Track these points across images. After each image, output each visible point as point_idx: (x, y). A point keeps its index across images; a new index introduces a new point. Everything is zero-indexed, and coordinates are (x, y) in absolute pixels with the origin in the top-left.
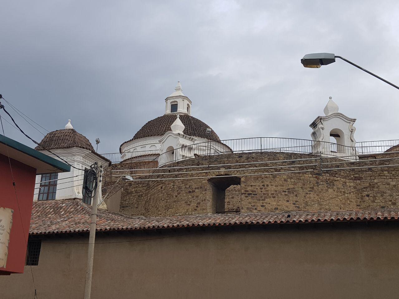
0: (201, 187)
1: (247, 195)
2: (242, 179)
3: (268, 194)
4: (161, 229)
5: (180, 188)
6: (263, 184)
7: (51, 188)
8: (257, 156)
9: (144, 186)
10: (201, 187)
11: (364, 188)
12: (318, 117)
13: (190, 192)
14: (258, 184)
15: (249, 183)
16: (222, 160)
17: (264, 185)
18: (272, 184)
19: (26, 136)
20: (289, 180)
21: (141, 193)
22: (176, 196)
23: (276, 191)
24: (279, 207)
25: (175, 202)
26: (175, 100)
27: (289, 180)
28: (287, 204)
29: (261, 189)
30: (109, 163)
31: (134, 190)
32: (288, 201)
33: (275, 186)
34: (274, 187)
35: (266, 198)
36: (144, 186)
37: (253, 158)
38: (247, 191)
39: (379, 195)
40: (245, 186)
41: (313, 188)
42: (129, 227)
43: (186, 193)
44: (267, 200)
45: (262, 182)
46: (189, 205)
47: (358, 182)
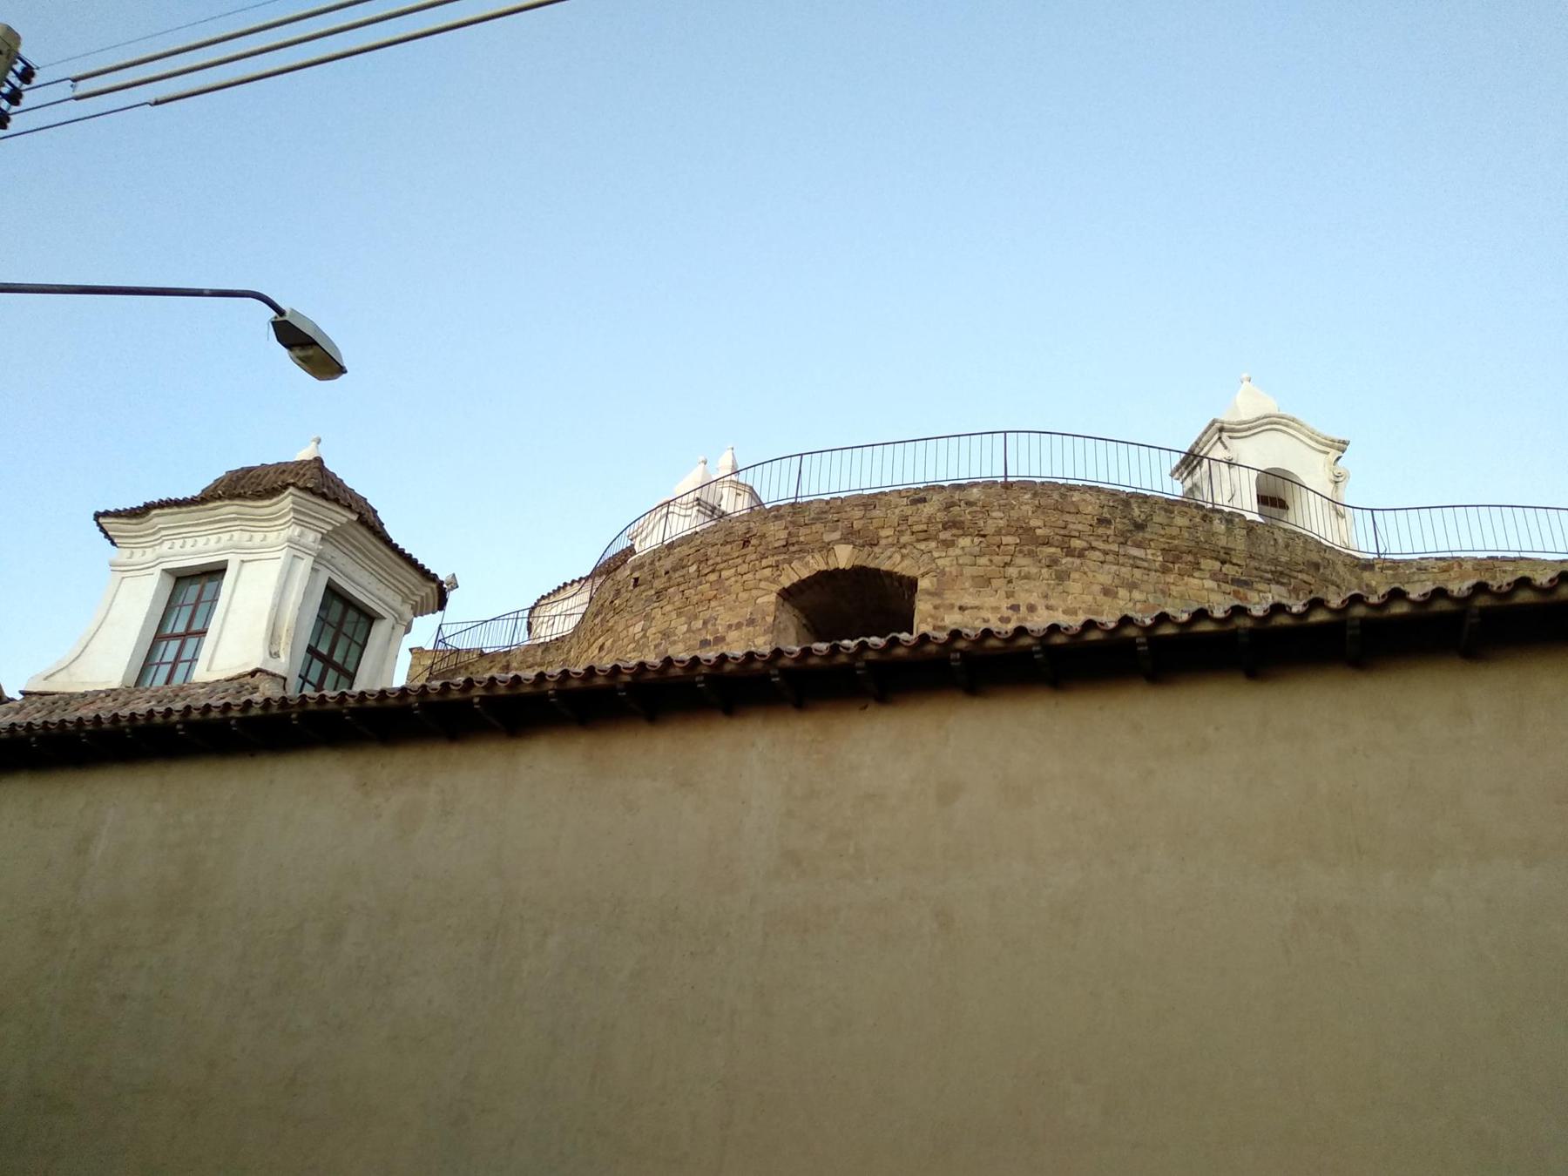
0: (751, 622)
2: (923, 584)
6: (1012, 601)
7: (191, 642)
8: (988, 496)
10: (751, 622)
12: (1214, 422)
14: (991, 601)
15: (950, 597)
16: (844, 515)
17: (1015, 608)
18: (1052, 602)
20: (1122, 592)
27: (1122, 592)
33: (1064, 612)
37: (969, 504)
40: (936, 607)
45: (1009, 595)
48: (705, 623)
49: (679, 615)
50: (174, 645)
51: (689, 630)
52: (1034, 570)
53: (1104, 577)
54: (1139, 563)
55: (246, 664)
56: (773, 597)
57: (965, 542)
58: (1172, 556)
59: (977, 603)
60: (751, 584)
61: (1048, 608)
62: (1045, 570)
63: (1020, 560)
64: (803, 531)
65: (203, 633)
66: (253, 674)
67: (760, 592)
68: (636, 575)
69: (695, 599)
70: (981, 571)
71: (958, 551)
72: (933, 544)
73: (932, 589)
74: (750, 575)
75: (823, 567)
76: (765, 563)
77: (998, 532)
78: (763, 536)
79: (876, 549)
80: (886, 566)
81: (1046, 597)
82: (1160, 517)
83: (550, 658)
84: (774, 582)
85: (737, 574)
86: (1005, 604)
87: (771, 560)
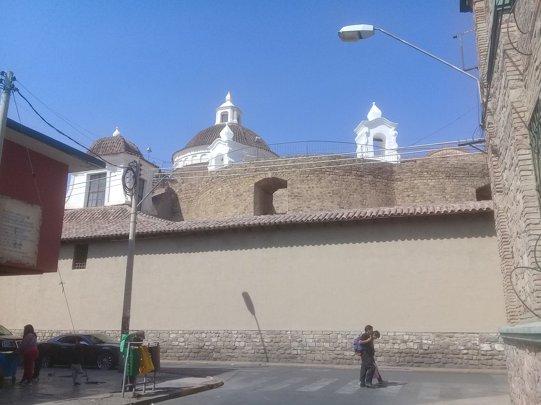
0: (249, 191)
1: (293, 197)
2: (288, 182)
3: (314, 197)
4: (208, 230)
5: (228, 192)
6: (309, 186)
10: (249, 191)
11: (405, 189)
13: (238, 196)
14: (304, 186)
17: (309, 188)
19: (49, 124)
21: (191, 199)
22: (225, 200)
23: (321, 193)
24: (324, 209)
25: (223, 205)
26: (226, 110)
28: (332, 205)
29: (307, 191)
31: (184, 196)
32: (333, 202)
35: (311, 199)
39: (418, 195)
41: (356, 189)
42: (176, 229)
44: (313, 202)
46: (237, 208)
47: (399, 183)
50: (95, 195)
51: (233, 192)
53: (329, 178)
66: (123, 205)
69: (234, 183)
75: (265, 177)
81: (316, 185)
83: (193, 188)
84: (254, 180)
86: (307, 186)
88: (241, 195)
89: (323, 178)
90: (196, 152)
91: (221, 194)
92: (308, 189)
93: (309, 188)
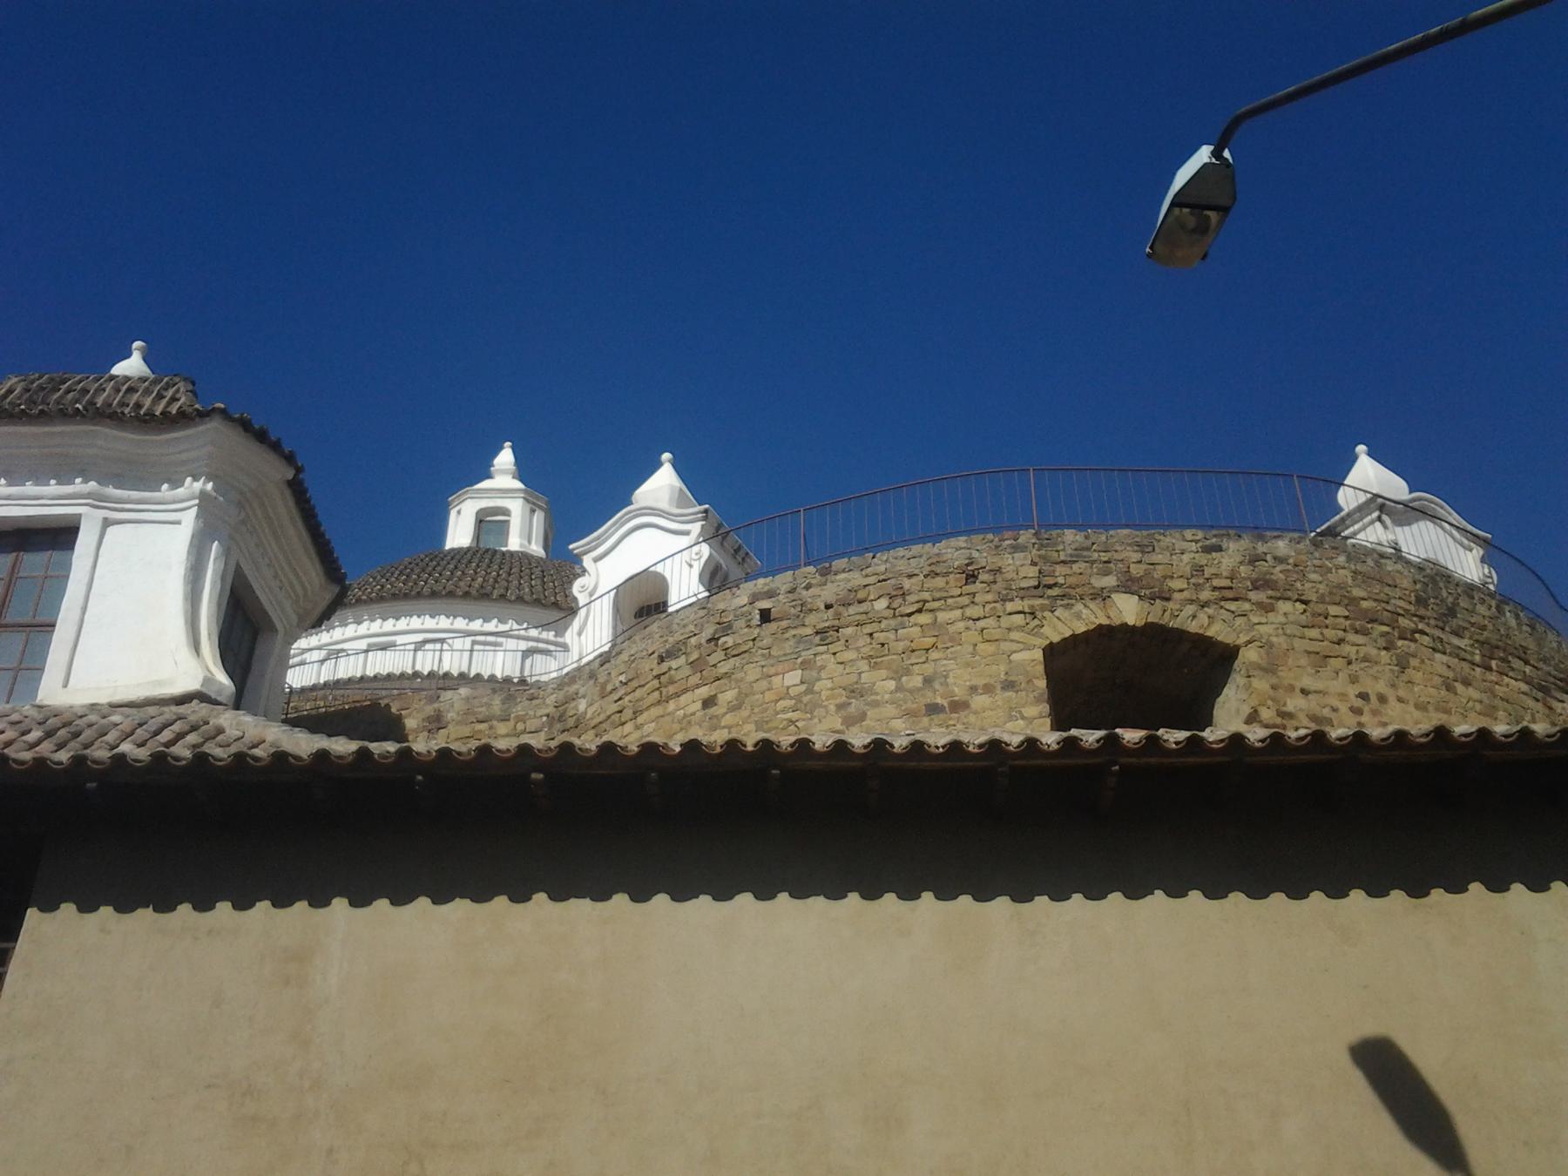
2: (1249, 655)
5: (855, 691)
9: (524, 732)
10: (1009, 685)
13: (933, 709)
14: (1337, 685)
15: (1286, 676)
18: (1401, 693)
20: (1459, 687)
30: (336, 589)
33: (1417, 706)
34: (1411, 708)
36: (524, 732)
37: (1279, 560)
38: (1290, 716)
40: (1274, 687)
43: (910, 714)
48: (928, 681)
49: (875, 667)
51: (899, 689)
52: (1374, 652)
54: (1463, 654)
55: (160, 683)
56: (1038, 655)
57: (1283, 606)
58: (1490, 650)
59: (1319, 686)
60: (997, 634)
61: (1400, 700)
62: (1383, 653)
63: (1351, 637)
64: (1059, 569)
65: (54, 626)
67: (1015, 646)
68: (765, 604)
70: (1316, 646)
71: (1282, 619)
72: (1247, 606)
73: (1264, 663)
74: (991, 622)
75: (1105, 622)
76: (1010, 607)
77: (1321, 600)
78: (999, 570)
79: (1170, 605)
80: (1193, 627)
81: (1393, 686)
82: (1464, 603)
85: (964, 618)
86: (1352, 691)
87: (1024, 605)
88: (958, 706)
89: (1414, 662)
90: (389, 625)
91: (806, 702)
92: (1359, 703)
93: (1363, 696)
